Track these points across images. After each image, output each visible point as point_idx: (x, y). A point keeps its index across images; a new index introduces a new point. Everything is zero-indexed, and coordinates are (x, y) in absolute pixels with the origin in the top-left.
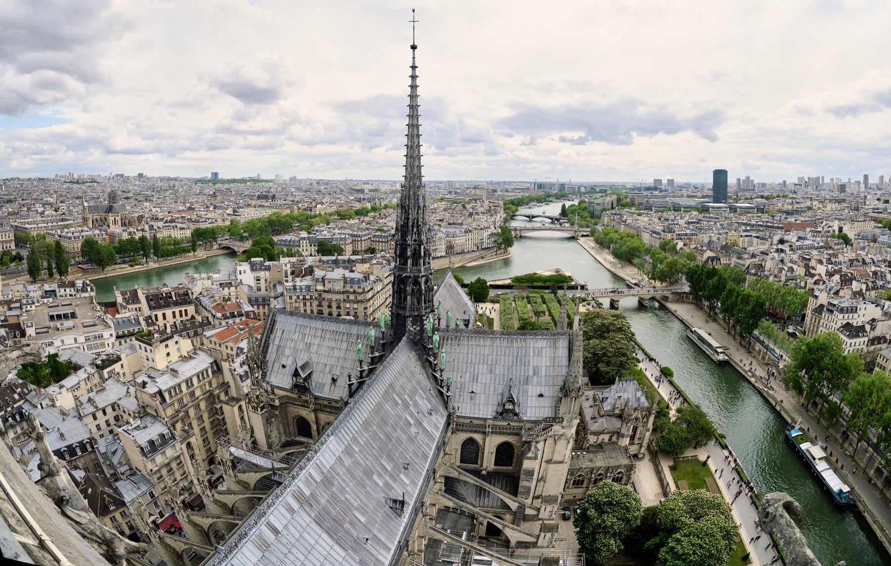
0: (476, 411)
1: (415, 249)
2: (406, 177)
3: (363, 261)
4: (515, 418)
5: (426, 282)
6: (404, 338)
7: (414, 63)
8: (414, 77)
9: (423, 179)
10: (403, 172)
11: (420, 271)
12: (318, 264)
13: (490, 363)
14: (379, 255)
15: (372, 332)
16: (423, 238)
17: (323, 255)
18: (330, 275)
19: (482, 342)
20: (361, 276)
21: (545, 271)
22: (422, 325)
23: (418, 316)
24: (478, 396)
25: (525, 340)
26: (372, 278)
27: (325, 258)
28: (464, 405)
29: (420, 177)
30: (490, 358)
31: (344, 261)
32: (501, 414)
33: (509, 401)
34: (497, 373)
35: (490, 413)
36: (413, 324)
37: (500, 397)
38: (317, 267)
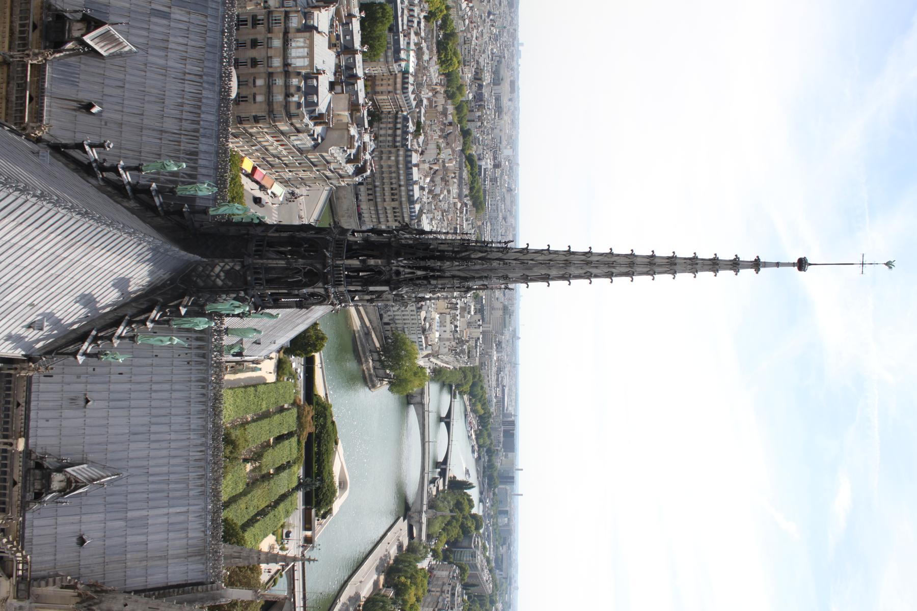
0: (42, 414)
1: (380, 273)
2: (525, 251)
3: (354, 107)
4: (30, 496)
5: (312, 295)
6: (198, 258)
7: (766, 265)
8: (735, 265)
9: (522, 287)
10: (537, 244)
11: (337, 284)
12: (344, 13)
13: (154, 428)
14: (366, 138)
15: (204, 190)
16: (404, 291)
17: (362, 21)
18: (321, 43)
19: (195, 408)
20: (322, 108)
21: (339, 464)
22: (226, 290)
23: (246, 283)
24: (79, 413)
25: (203, 493)
26: (319, 129)
27: (356, 25)
28: (57, 387)
29: (526, 279)
30: (165, 428)
31: (351, 67)
32: (39, 466)
33: (69, 481)
34: (133, 446)
35: (41, 442)
36: (227, 273)
37: (78, 457)
38: (337, 12)
